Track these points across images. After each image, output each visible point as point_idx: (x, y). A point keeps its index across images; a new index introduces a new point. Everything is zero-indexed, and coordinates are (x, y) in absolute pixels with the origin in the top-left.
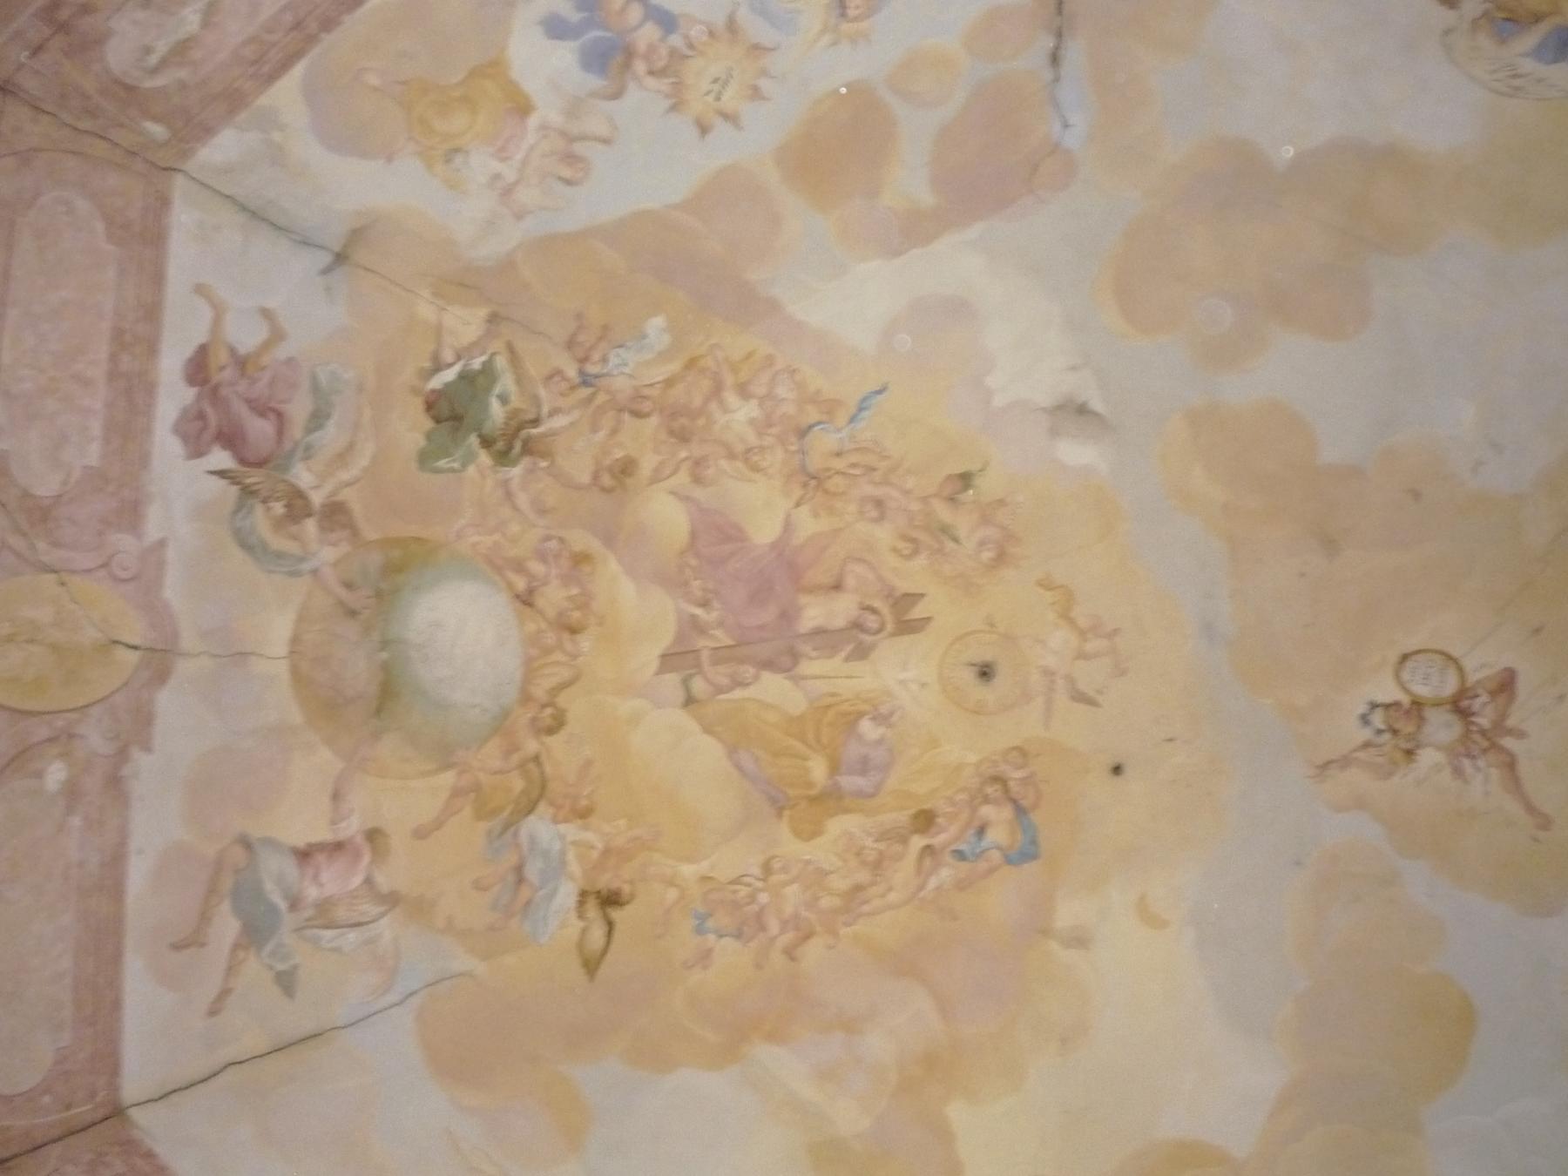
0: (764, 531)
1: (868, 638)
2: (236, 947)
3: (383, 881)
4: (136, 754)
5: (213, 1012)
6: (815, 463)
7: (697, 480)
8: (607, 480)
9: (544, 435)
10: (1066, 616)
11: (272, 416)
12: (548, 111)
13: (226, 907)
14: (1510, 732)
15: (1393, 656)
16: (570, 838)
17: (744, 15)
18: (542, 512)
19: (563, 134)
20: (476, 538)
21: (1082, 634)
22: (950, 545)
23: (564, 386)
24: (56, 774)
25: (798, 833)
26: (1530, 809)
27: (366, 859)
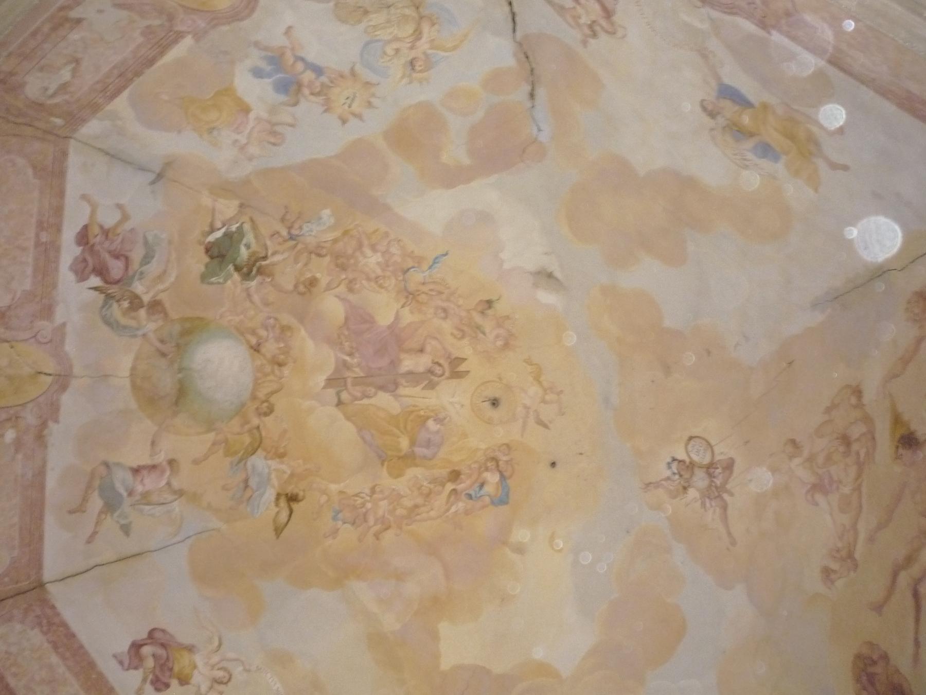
0: (384, 319)
1: (436, 379)
2: (101, 513)
3: (176, 484)
4: (51, 424)
5: (89, 542)
6: (412, 287)
7: (351, 290)
8: (302, 288)
9: (267, 265)
10: (537, 379)
11: (123, 259)
12: (259, 110)
13: (96, 493)
14: (727, 491)
15: (686, 438)
16: (273, 468)
17: (358, 68)
18: (267, 304)
19: (269, 122)
20: (230, 318)
21: (545, 390)
22: (481, 335)
23: (280, 240)
24: (10, 435)
25: (390, 474)
26: (729, 534)
27: (168, 473)
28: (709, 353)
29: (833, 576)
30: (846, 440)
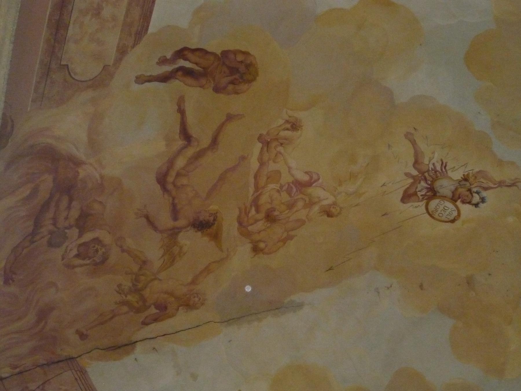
14: (413, 177)
15: (458, 223)
26: (414, 143)
28: (421, 287)
29: (288, 126)
30: (270, 218)
